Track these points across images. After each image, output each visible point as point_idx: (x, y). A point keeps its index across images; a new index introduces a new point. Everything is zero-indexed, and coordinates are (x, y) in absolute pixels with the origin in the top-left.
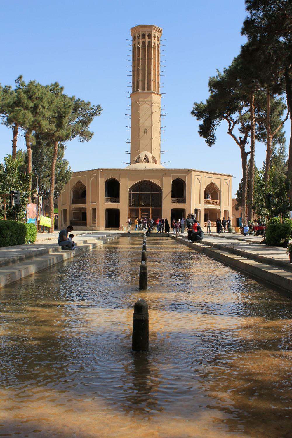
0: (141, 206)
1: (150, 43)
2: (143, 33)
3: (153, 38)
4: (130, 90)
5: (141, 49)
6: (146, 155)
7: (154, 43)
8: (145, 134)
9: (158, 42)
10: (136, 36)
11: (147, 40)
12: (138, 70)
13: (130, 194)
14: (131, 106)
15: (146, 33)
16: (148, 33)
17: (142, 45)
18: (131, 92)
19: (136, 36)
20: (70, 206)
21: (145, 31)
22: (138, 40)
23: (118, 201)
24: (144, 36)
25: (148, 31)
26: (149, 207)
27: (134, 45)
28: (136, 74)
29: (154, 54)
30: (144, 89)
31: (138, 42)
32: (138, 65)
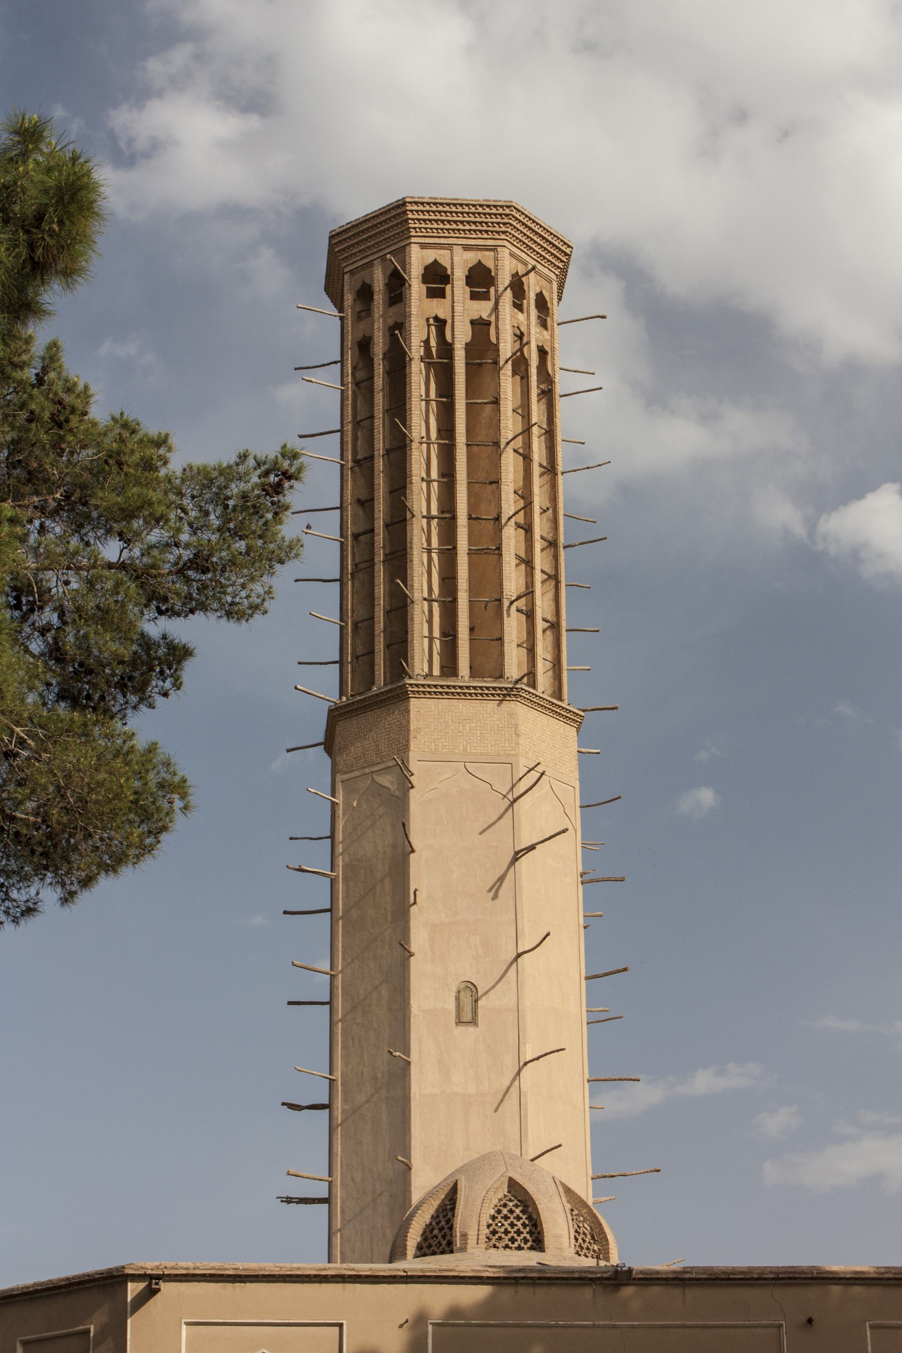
2: (431, 256)
3: (508, 296)
6: (513, 1185)
8: (459, 1022)
9: (546, 335)
11: (458, 308)
16: (472, 258)
21: (450, 247)
28: (380, 556)
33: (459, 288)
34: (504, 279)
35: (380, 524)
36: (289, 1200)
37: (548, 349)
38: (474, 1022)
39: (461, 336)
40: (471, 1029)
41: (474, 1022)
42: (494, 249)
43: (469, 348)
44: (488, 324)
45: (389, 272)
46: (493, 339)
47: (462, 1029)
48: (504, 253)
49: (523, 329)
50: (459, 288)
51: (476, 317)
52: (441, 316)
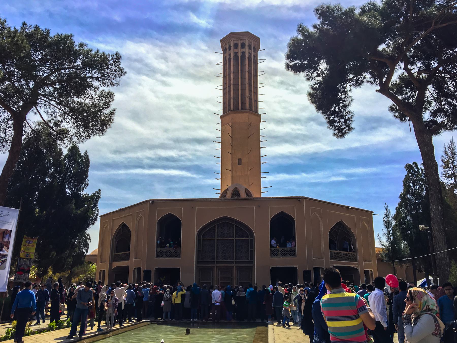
0: (218, 263)
1: (243, 53)
2: (235, 42)
3: (247, 47)
4: (221, 113)
5: (232, 61)
6: (236, 188)
7: (249, 53)
8: (238, 165)
9: (255, 54)
10: (227, 48)
11: (240, 50)
12: (229, 87)
13: (199, 241)
14: (222, 131)
15: (239, 42)
16: (242, 41)
17: (233, 56)
18: (222, 114)
19: (227, 48)
20: (111, 265)
22: (229, 52)
23: (178, 255)
24: (236, 46)
25: (241, 40)
26: (232, 265)
27: (225, 59)
28: (227, 92)
29: (250, 66)
30: (236, 108)
31: (229, 53)
32: (230, 81)
33: (239, 47)
34: (247, 44)
35: (227, 86)
36: (217, 193)
37: (255, 56)
38: (241, 164)
39: (240, 55)
40: (241, 165)
41: (241, 164)
42: (245, 40)
43: (241, 57)
44: (244, 52)
45: (229, 45)
46: (245, 55)
47: (239, 166)
48: (247, 41)
49: (251, 53)
50: (239, 47)
51: (242, 51)
52: (237, 52)
